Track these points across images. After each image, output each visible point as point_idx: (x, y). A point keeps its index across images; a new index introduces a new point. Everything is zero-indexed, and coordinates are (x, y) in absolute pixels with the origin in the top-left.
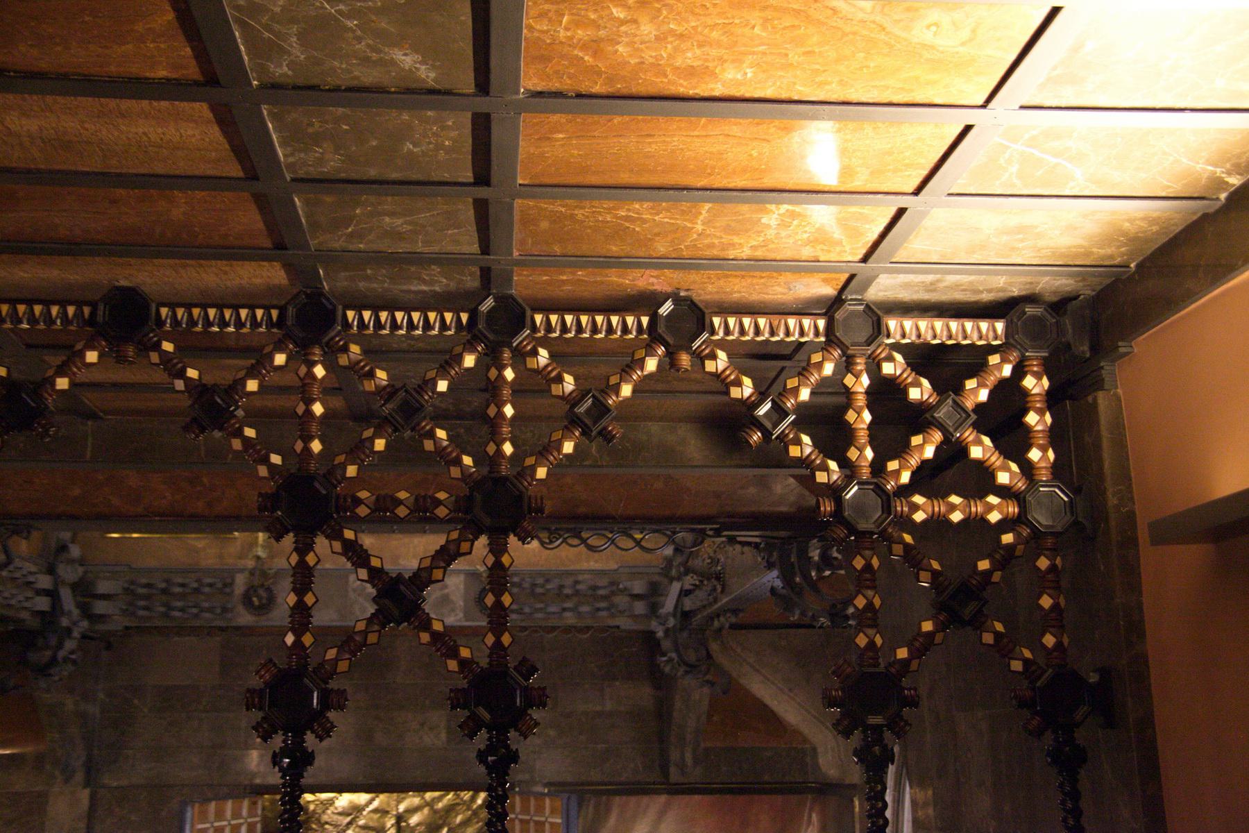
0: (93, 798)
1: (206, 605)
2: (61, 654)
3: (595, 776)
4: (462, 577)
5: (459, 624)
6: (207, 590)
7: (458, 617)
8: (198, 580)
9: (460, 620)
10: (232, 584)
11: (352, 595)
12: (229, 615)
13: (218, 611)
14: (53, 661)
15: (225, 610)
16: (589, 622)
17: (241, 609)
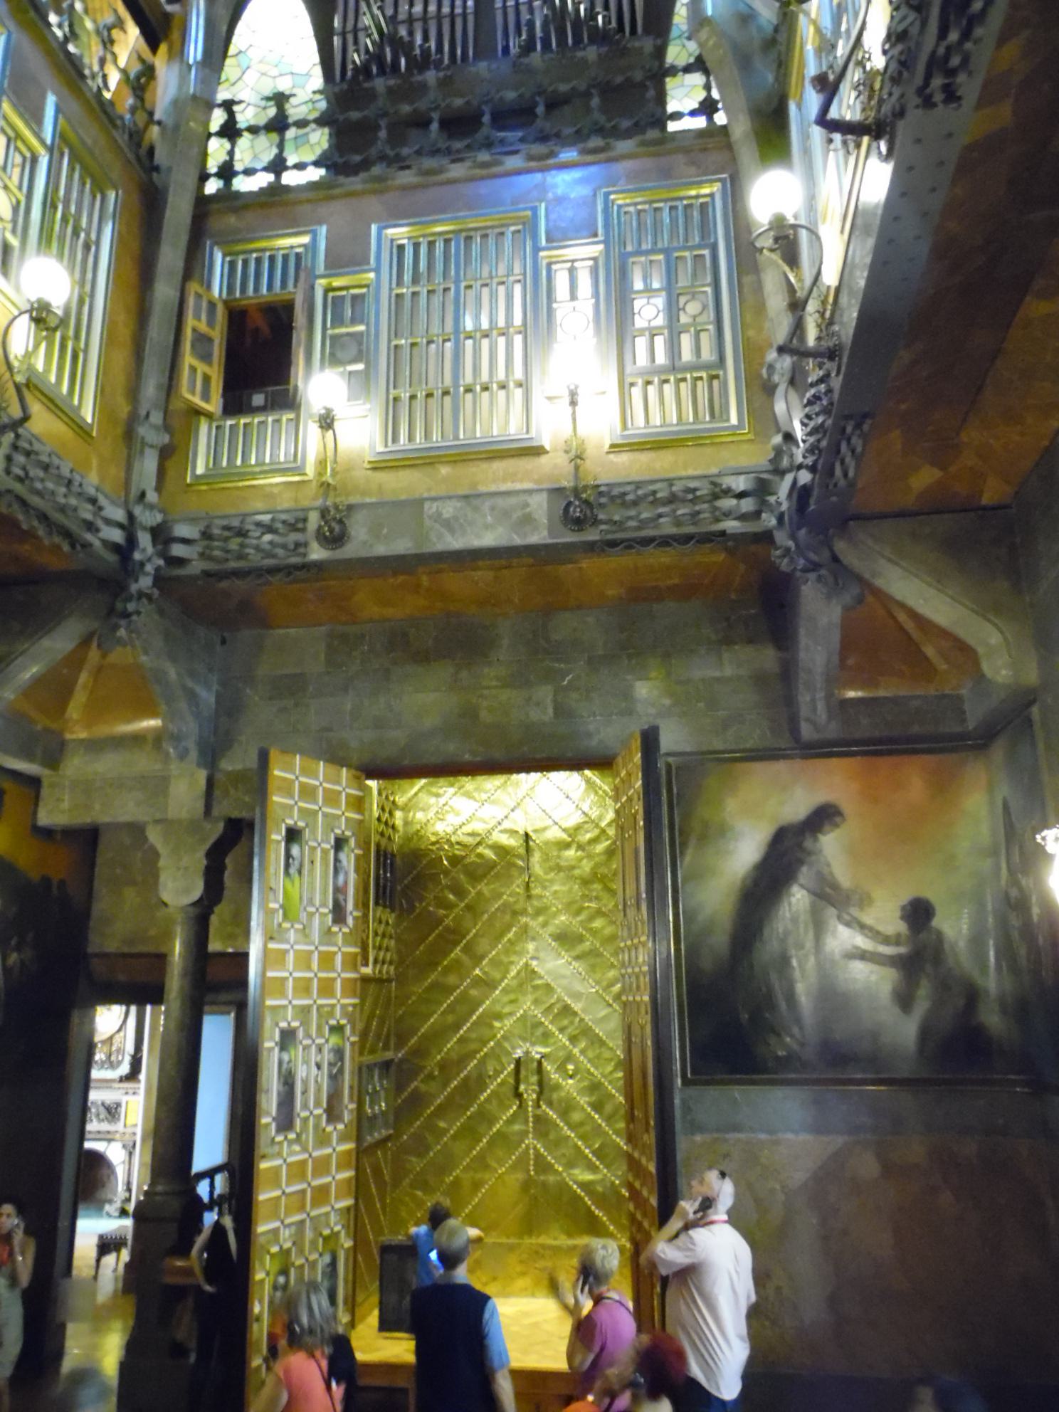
3: (718, 744)
4: (545, 495)
5: (544, 542)
7: (542, 535)
9: (544, 538)
10: (305, 520)
11: (428, 522)
12: (302, 550)
17: (315, 545)
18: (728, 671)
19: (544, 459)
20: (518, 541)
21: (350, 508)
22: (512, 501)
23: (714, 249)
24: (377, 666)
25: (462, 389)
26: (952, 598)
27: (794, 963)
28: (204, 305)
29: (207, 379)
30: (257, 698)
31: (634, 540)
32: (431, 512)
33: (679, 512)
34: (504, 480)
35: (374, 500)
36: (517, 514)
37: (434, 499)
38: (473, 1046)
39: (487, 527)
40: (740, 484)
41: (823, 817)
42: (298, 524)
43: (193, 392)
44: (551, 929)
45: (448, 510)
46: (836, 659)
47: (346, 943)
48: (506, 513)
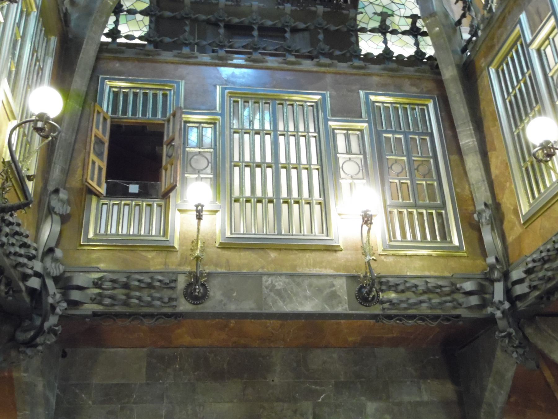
7: (344, 308)
8: (152, 278)
9: (346, 310)
10: (175, 281)
11: (265, 291)
12: (174, 303)
16: (438, 312)
17: (183, 300)
18: (426, 398)
19: (339, 254)
20: (328, 310)
21: (209, 274)
22: (323, 281)
23: (431, 135)
24: (186, 381)
25: (282, 201)
28: (101, 119)
29: (100, 169)
30: (90, 402)
31: (403, 316)
32: (267, 284)
33: (433, 301)
34: (314, 266)
35: (223, 270)
37: (270, 275)
39: (306, 298)
40: (469, 286)
42: (170, 285)
43: (92, 179)
45: (280, 283)
48: (319, 290)
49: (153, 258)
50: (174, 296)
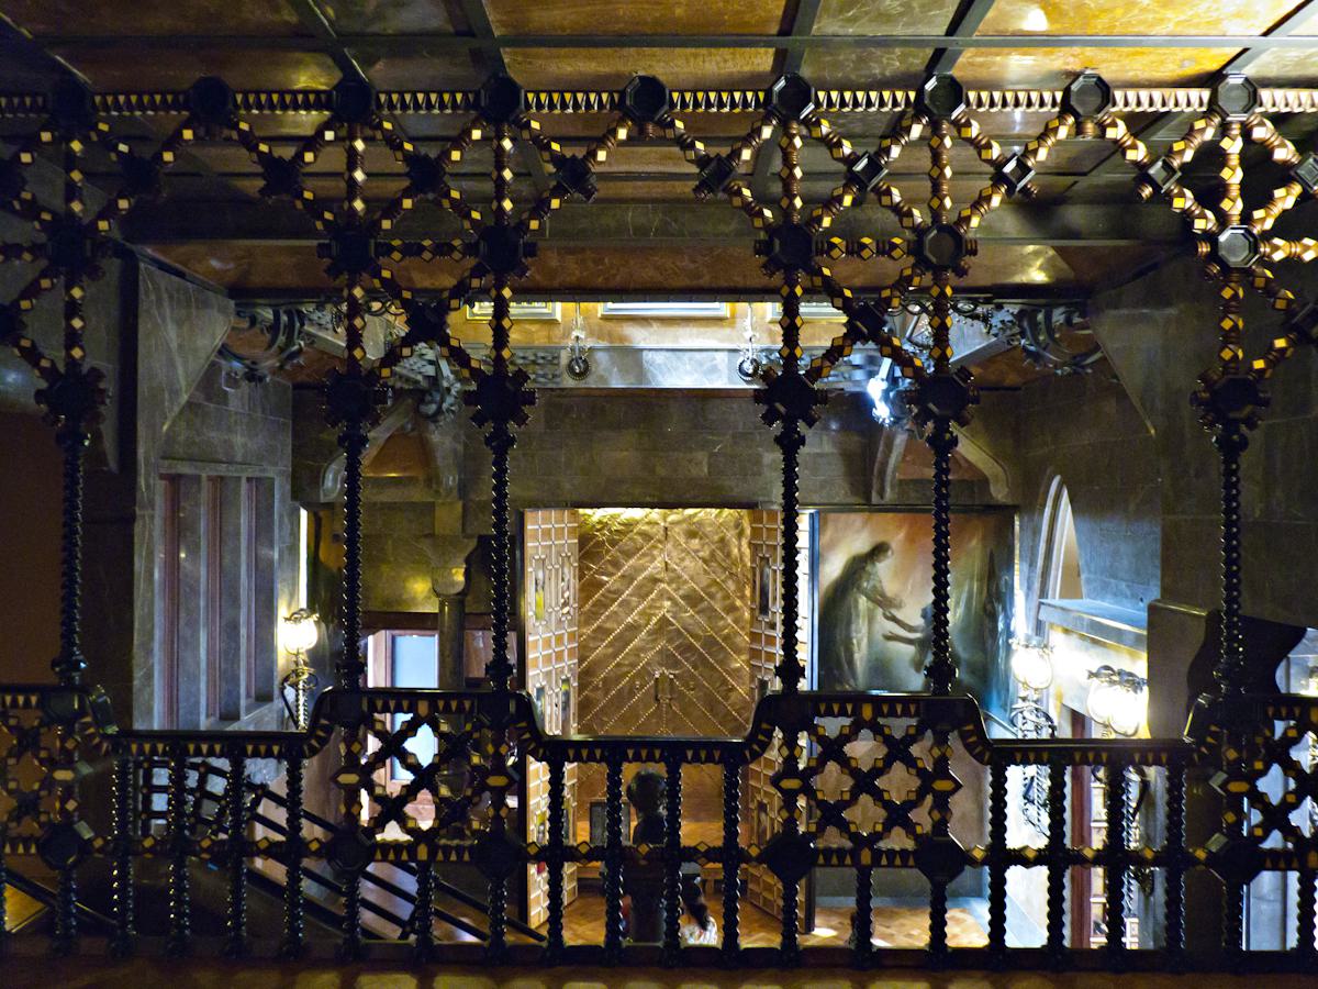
0: (465, 508)
1: (541, 372)
2: (445, 406)
6: (541, 361)
8: (535, 355)
10: (558, 357)
12: (558, 380)
13: (550, 376)
14: (439, 411)
15: (554, 376)
26: (979, 447)
27: (855, 641)
36: (708, 364)
38: (625, 669)
41: (878, 551)
44: (681, 592)
46: (900, 458)
47: (570, 626)
49: (537, 332)
50: (557, 373)
